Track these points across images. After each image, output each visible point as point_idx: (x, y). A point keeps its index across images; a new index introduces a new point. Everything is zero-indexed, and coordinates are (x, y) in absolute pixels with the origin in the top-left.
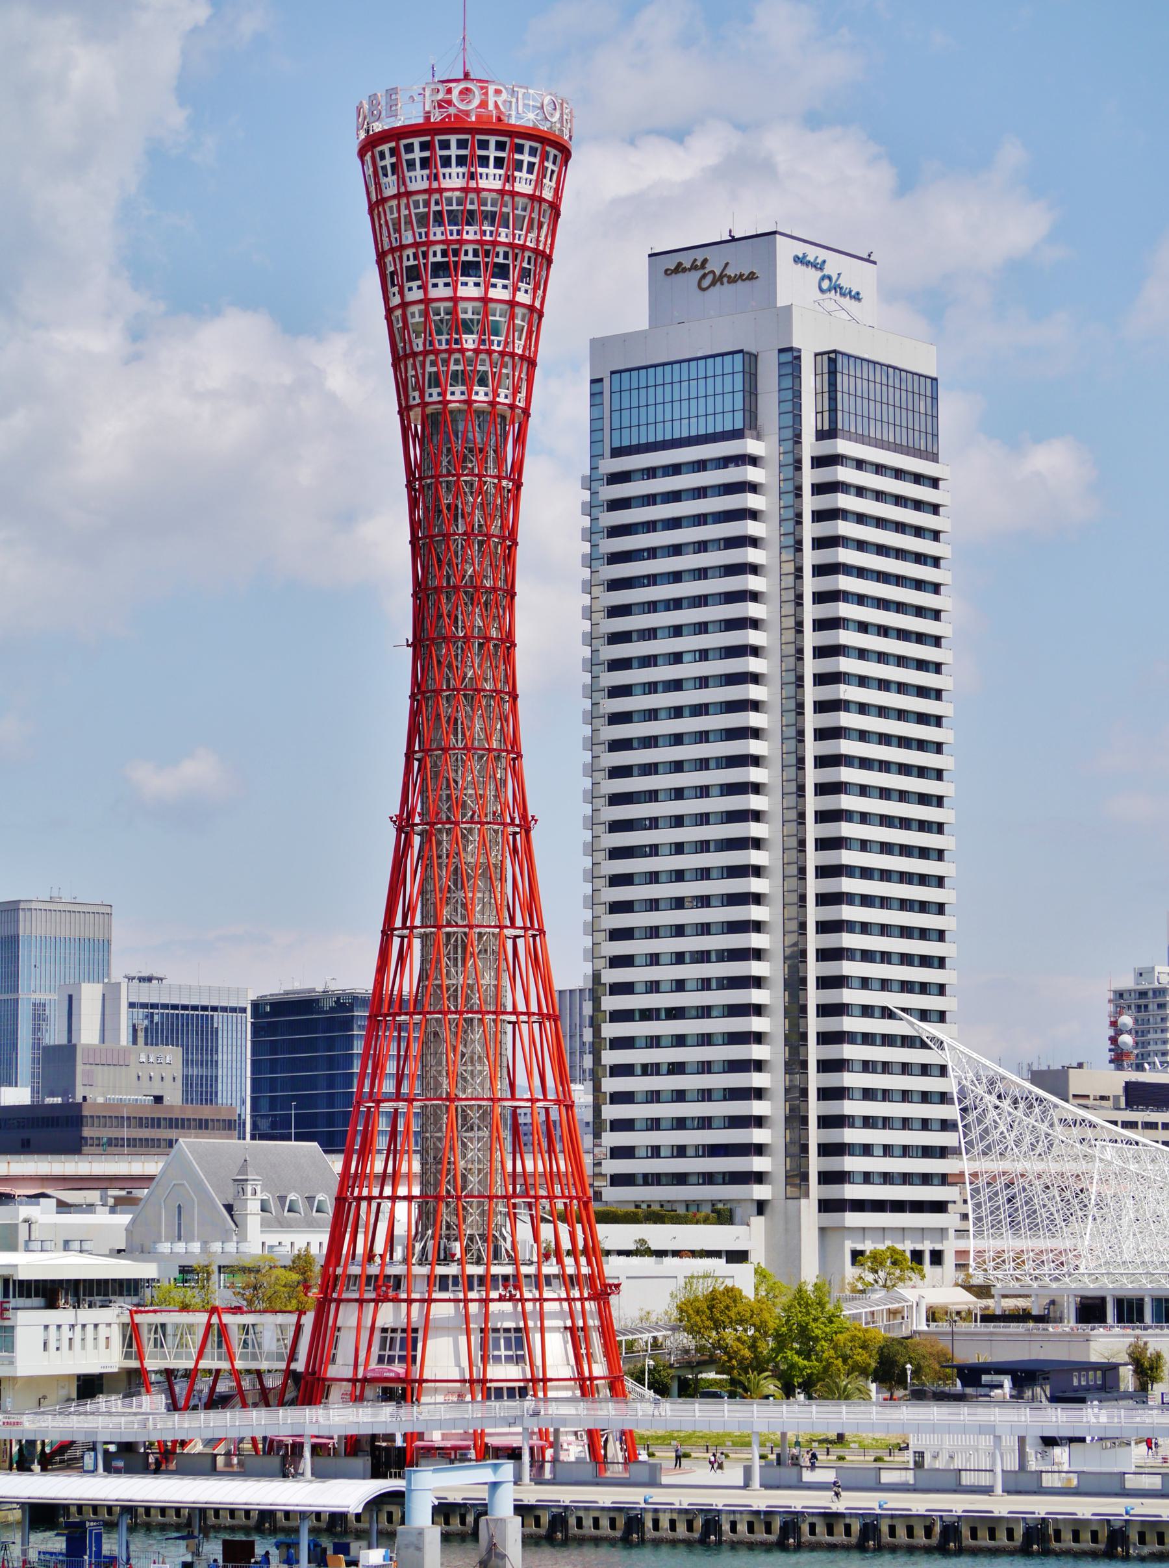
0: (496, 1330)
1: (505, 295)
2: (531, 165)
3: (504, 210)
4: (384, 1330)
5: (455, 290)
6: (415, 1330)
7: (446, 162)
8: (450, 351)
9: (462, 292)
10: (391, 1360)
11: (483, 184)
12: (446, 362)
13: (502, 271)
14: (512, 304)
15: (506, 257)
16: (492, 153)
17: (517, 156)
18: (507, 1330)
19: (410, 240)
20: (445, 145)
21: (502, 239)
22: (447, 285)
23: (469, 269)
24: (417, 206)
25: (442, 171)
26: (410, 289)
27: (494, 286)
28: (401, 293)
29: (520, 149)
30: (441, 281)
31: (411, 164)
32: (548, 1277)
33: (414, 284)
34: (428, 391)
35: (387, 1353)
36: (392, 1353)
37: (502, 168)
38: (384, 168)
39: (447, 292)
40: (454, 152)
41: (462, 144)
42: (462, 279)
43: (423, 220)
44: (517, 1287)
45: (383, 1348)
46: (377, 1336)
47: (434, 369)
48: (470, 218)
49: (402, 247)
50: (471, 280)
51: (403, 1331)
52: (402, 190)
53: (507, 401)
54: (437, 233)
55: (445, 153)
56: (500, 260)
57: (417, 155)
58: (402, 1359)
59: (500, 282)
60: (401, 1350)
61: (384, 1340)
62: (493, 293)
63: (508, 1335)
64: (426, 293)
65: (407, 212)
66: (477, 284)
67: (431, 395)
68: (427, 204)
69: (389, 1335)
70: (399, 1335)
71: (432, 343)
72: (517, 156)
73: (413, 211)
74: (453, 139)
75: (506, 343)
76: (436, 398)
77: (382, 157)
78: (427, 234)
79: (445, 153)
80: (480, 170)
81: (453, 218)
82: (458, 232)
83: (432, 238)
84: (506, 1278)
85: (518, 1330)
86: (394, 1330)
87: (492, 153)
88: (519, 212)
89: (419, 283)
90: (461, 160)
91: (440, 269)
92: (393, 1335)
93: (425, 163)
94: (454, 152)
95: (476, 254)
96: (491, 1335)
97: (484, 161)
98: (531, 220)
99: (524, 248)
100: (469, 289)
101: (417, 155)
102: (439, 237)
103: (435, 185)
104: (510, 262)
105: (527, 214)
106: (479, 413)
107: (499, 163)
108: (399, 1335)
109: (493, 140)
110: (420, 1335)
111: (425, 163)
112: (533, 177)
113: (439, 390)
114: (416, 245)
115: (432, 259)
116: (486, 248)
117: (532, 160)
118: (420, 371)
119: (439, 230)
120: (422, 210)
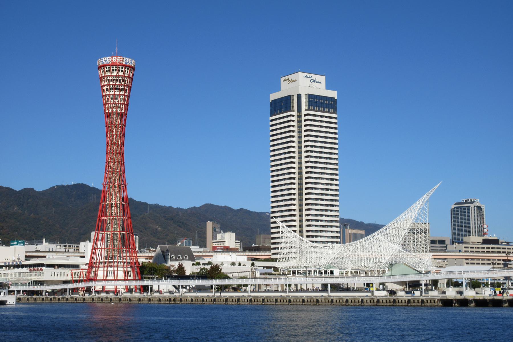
1: (123, 93)
2: (128, 71)
5: (114, 93)
7: (113, 70)
8: (113, 103)
9: (116, 93)
12: (112, 105)
13: (122, 89)
14: (124, 95)
15: (123, 87)
16: (121, 69)
20: (113, 68)
21: (123, 84)
23: (117, 89)
24: (108, 78)
29: (125, 68)
31: (107, 71)
33: (107, 91)
38: (102, 71)
39: (113, 93)
41: (116, 67)
43: (109, 80)
48: (117, 80)
50: (117, 91)
55: (113, 69)
56: (122, 87)
57: (108, 69)
68: (110, 78)
71: (110, 101)
74: (114, 67)
76: (111, 111)
77: (102, 69)
79: (113, 69)
81: (114, 80)
87: (121, 69)
90: (115, 70)
91: (111, 89)
94: (114, 69)
95: (118, 86)
97: (119, 71)
100: (117, 92)
101: (108, 69)
103: (111, 74)
104: (124, 88)
105: (127, 79)
106: (117, 113)
107: (122, 71)
111: (109, 71)
112: (128, 73)
115: (110, 87)
116: (119, 85)
119: (112, 82)
120: (109, 78)
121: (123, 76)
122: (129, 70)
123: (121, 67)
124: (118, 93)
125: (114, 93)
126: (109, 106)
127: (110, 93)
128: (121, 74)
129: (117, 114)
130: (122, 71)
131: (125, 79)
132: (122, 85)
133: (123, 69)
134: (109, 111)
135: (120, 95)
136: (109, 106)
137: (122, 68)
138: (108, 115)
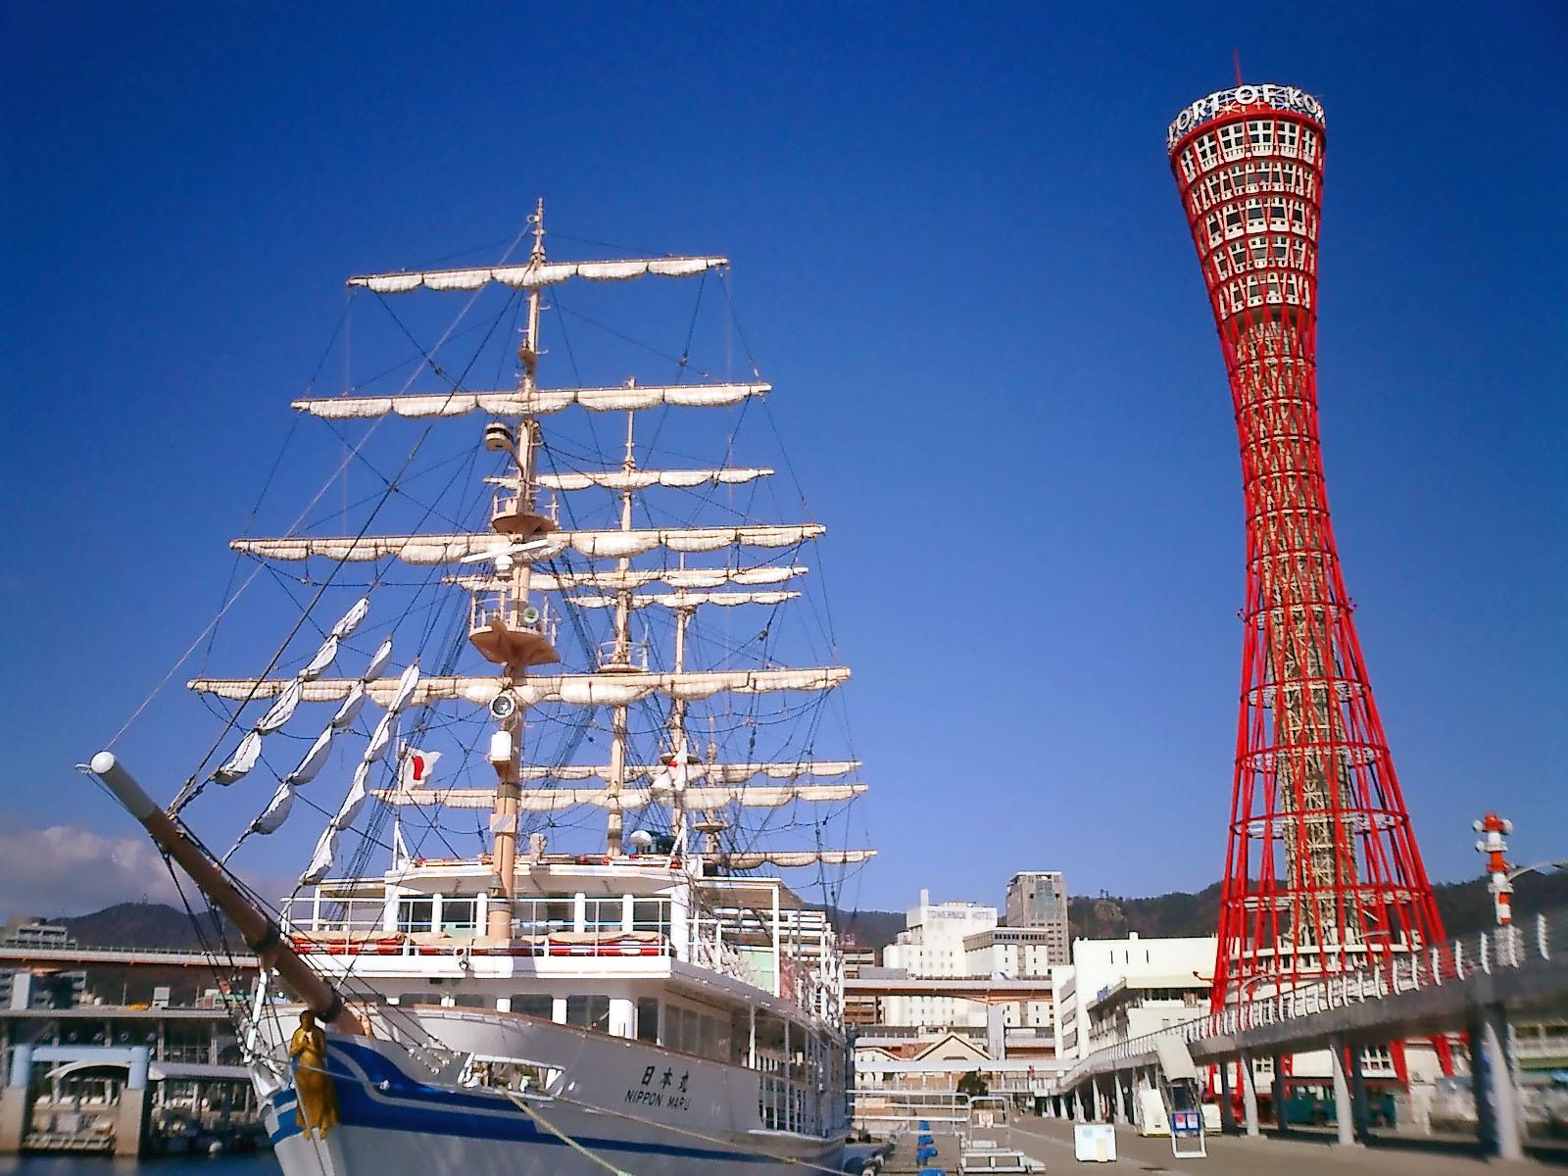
3: (1275, 170)
11: (1256, 153)
17: (1280, 133)
19: (1229, 196)
22: (1238, 228)
23: (1278, 212)
25: (1253, 145)
26: (1231, 231)
27: (1294, 225)
28: (1222, 235)
30: (1256, 222)
33: (1234, 227)
34: (1250, 299)
37: (1269, 141)
40: (1261, 132)
42: (1273, 219)
43: (1240, 181)
47: (1237, 289)
49: (1223, 203)
52: (1221, 162)
53: (1278, 302)
54: (1252, 189)
59: (1297, 223)
62: (1273, 228)
64: (1245, 230)
65: (1226, 177)
66: (1283, 223)
67: (1252, 302)
72: (1280, 133)
73: (1231, 175)
75: (1289, 263)
78: (1244, 190)
80: (1280, 144)
82: (1244, 190)
83: (1247, 191)
88: (1287, 170)
89: (1239, 224)
91: (1255, 214)
93: (1238, 141)
94: (1261, 132)
98: (1298, 177)
99: (1295, 195)
102: (1253, 191)
109: (1260, 124)
111: (1238, 141)
113: (1241, 302)
114: (1234, 199)
115: (1248, 207)
117: (1292, 135)
118: (1242, 286)
121: (1272, 157)
122: (1296, 135)
123: (1287, 125)
124: (1286, 228)
125: (1268, 226)
126: (1245, 283)
127: (1250, 230)
128: (1262, 150)
129: (1282, 315)
130: (1267, 138)
131: (1283, 168)
132: (1272, 193)
133: (1271, 132)
134: (1250, 305)
135: (1270, 233)
136: (1250, 283)
137: (1266, 127)
138: (1233, 329)
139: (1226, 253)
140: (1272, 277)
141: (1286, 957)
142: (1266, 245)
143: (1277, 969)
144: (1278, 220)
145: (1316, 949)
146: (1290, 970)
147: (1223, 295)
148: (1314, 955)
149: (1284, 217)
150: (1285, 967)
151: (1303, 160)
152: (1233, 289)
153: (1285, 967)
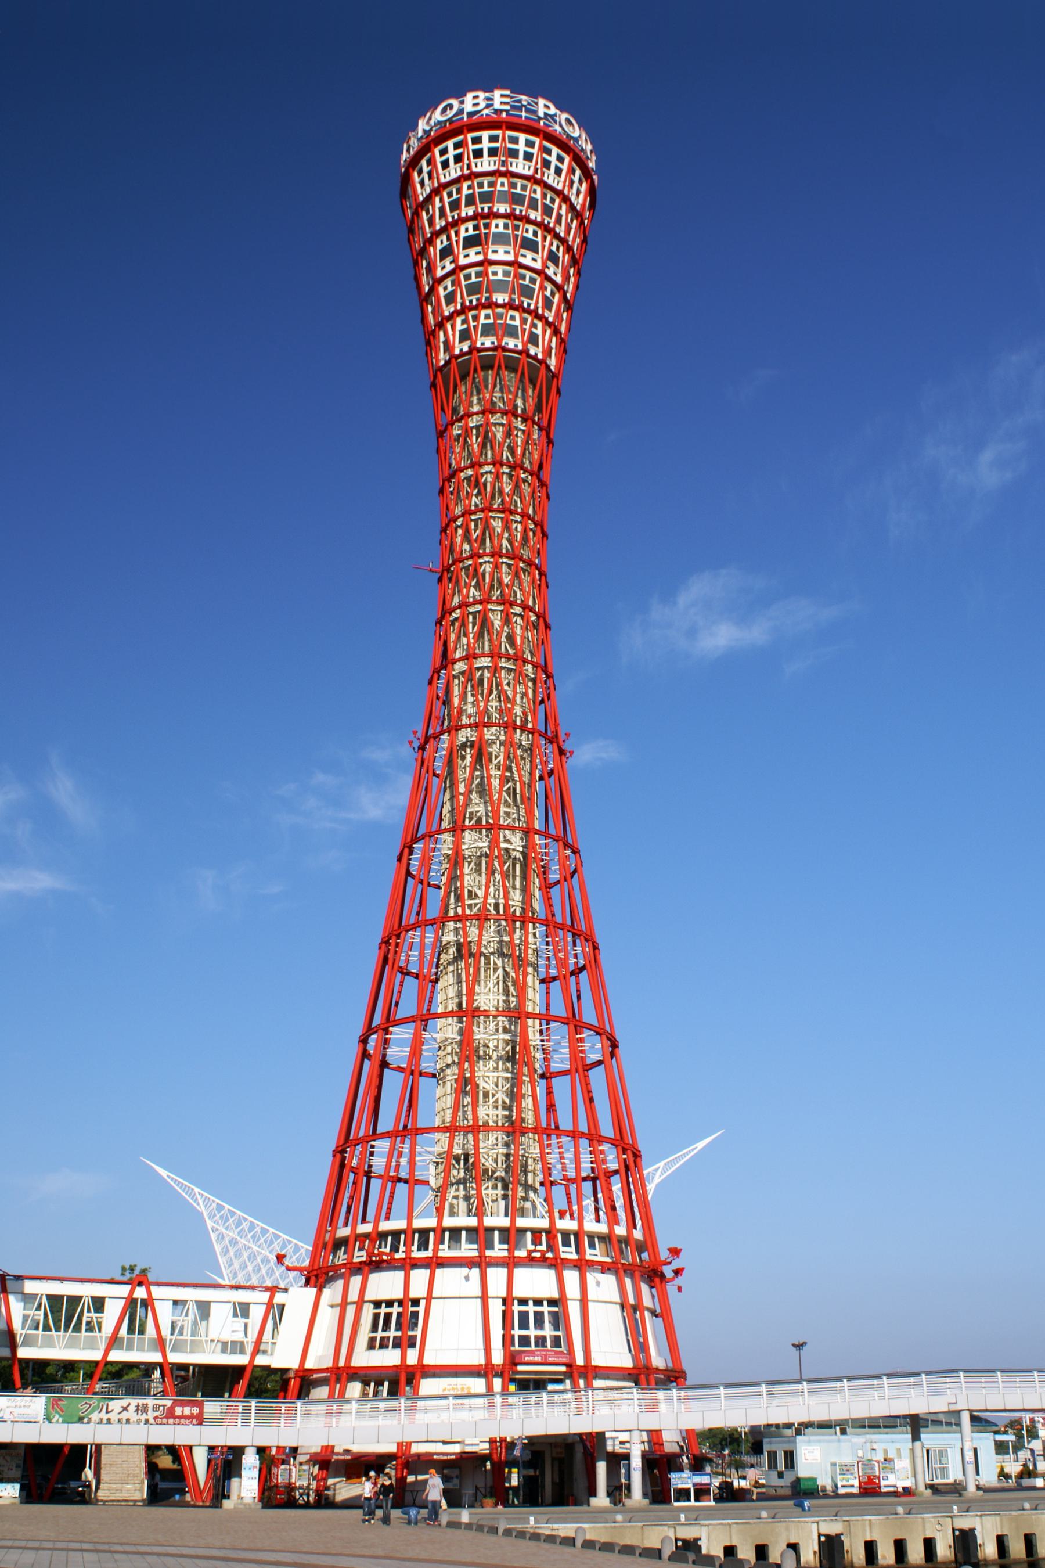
0: (523, 1302)
4: (377, 1304)
6: (416, 1302)
10: (383, 1345)
18: (538, 1302)
32: (591, 1237)
35: (380, 1334)
36: (385, 1334)
44: (551, 1247)
45: (374, 1328)
46: (368, 1311)
51: (401, 1303)
58: (397, 1344)
60: (397, 1330)
61: (376, 1317)
63: (539, 1309)
69: (383, 1310)
70: (395, 1310)
84: (536, 1233)
85: (552, 1302)
86: (390, 1303)
92: (389, 1310)
96: (516, 1308)
108: (395, 1310)
110: (421, 1309)
139: (456, 283)
140: (513, 318)
141: (424, 1233)
142: (510, 279)
143: (408, 1252)
144: (530, 255)
145: (473, 1222)
146: (429, 1254)
147: (446, 334)
148: (469, 1230)
149: (537, 253)
150: (419, 1250)
151: (568, 196)
152: (459, 327)
153: (419, 1250)
